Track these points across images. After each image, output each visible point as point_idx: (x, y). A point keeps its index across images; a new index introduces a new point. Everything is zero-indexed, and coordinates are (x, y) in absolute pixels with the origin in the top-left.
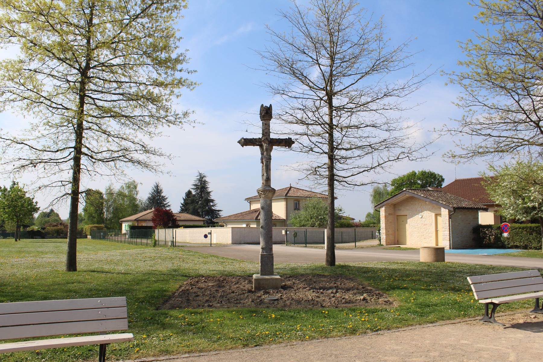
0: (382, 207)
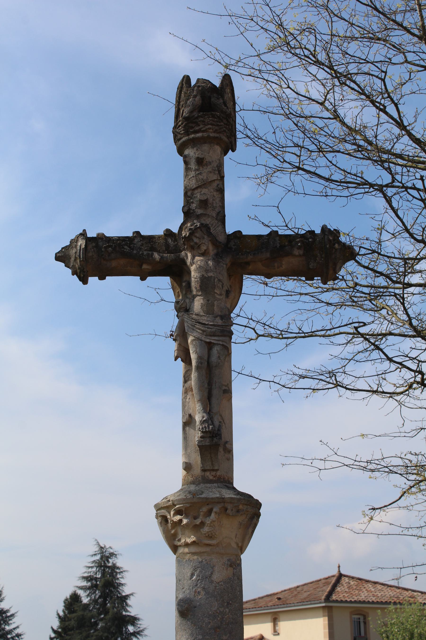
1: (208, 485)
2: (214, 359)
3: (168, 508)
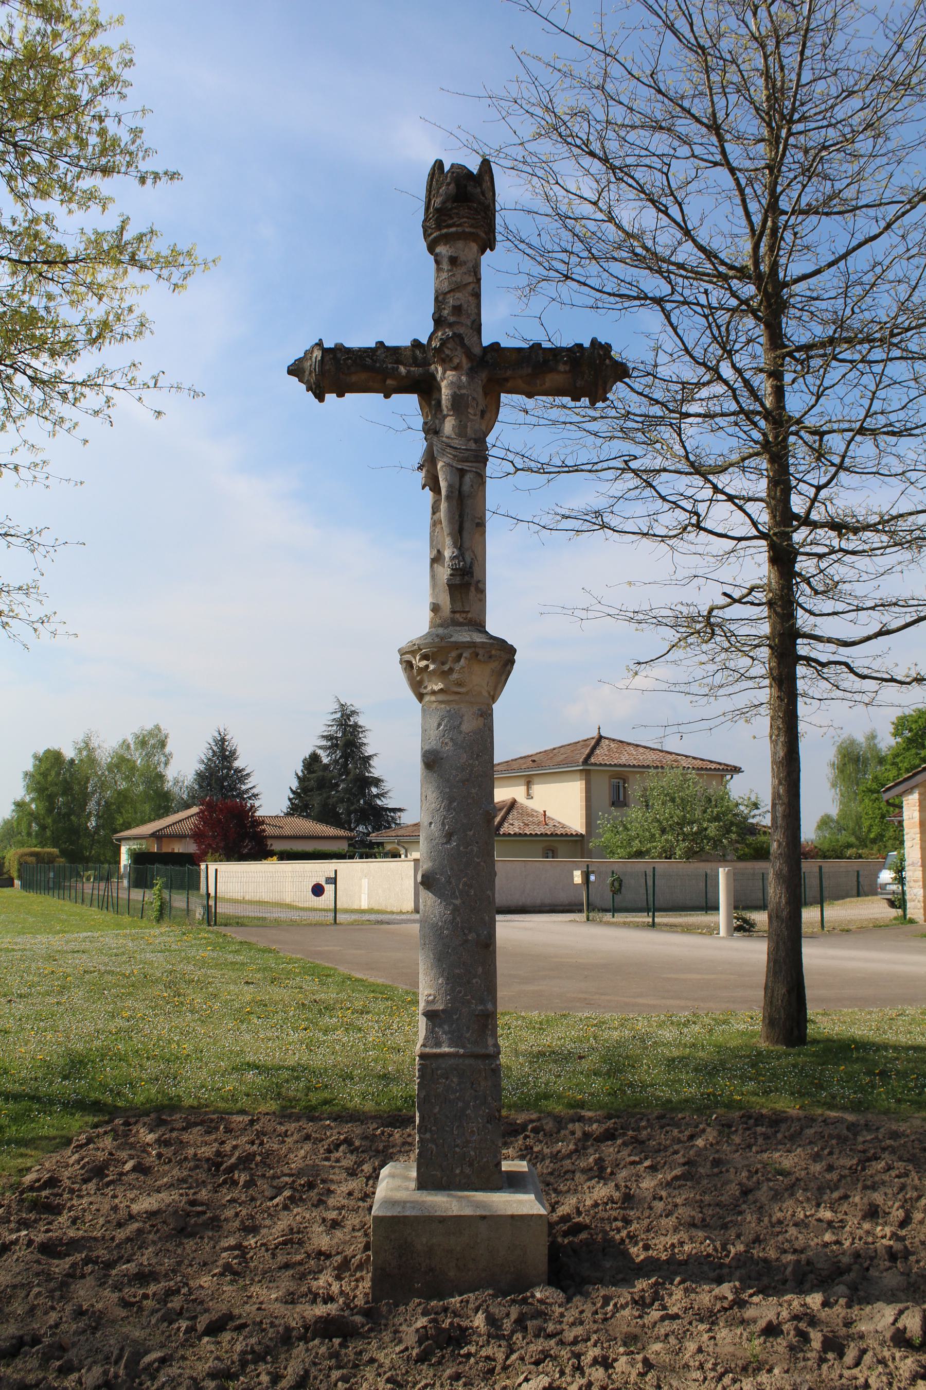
0: (910, 791)
1: (458, 628)
2: (466, 488)
3: (413, 653)
